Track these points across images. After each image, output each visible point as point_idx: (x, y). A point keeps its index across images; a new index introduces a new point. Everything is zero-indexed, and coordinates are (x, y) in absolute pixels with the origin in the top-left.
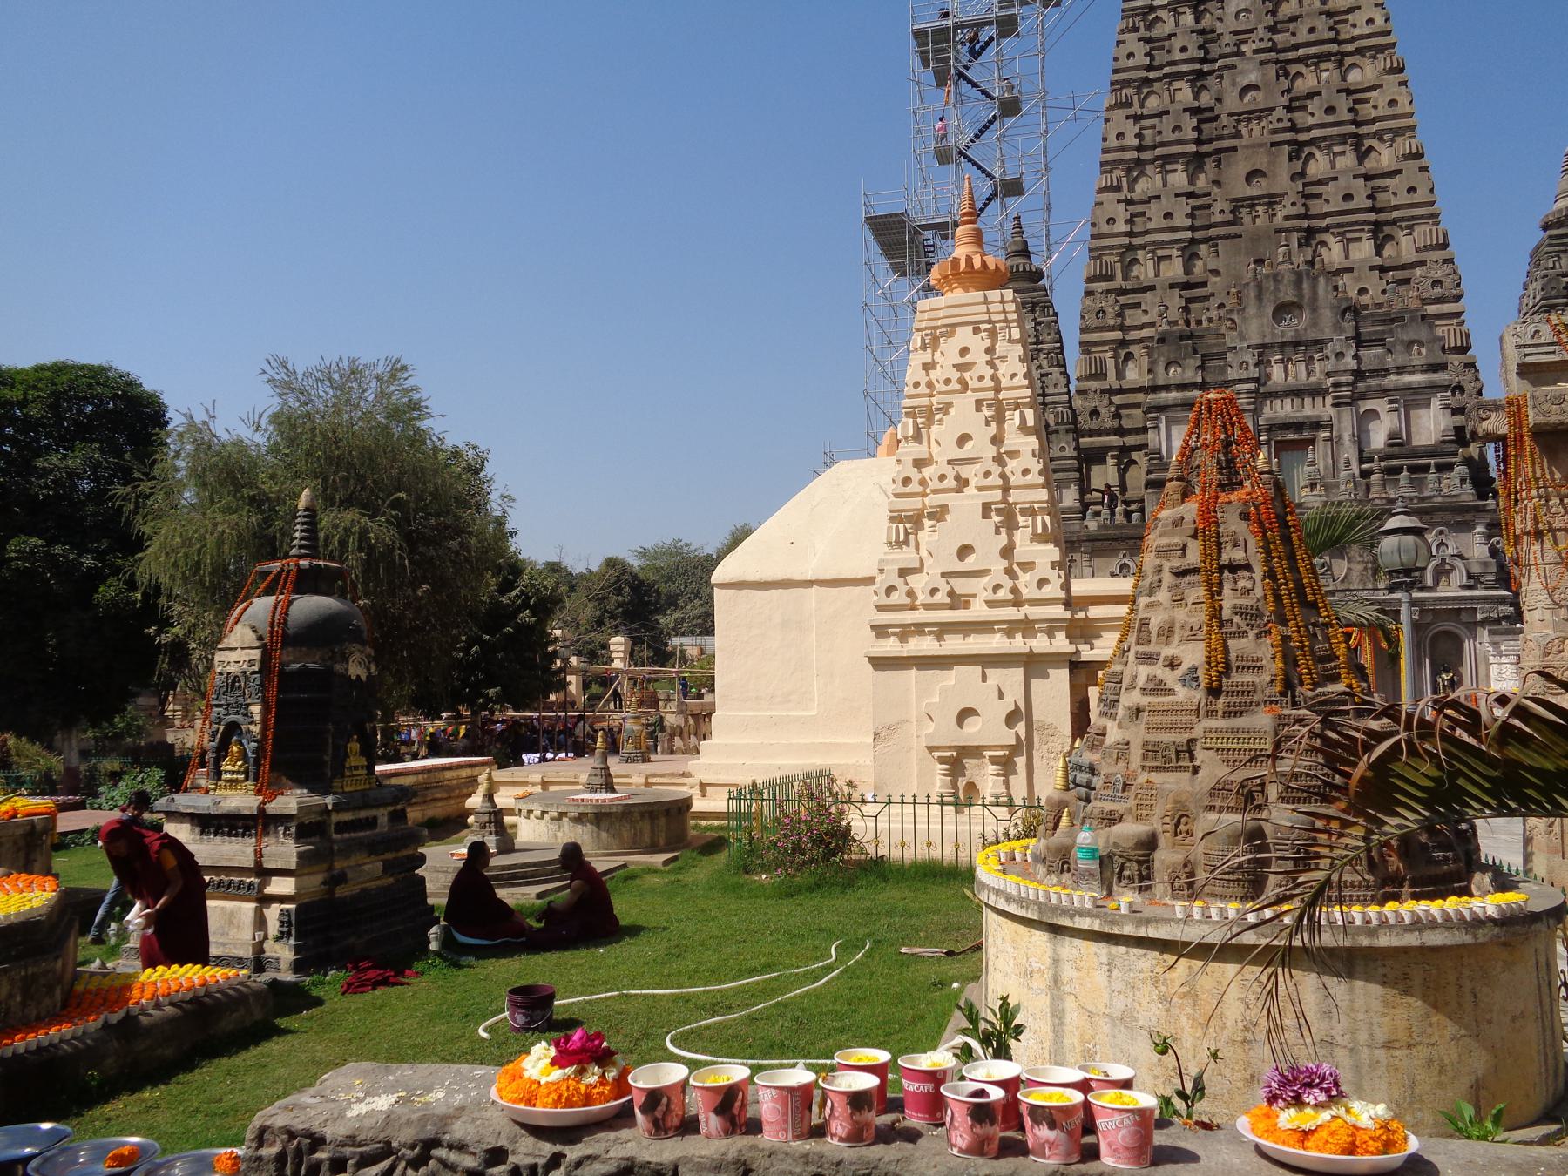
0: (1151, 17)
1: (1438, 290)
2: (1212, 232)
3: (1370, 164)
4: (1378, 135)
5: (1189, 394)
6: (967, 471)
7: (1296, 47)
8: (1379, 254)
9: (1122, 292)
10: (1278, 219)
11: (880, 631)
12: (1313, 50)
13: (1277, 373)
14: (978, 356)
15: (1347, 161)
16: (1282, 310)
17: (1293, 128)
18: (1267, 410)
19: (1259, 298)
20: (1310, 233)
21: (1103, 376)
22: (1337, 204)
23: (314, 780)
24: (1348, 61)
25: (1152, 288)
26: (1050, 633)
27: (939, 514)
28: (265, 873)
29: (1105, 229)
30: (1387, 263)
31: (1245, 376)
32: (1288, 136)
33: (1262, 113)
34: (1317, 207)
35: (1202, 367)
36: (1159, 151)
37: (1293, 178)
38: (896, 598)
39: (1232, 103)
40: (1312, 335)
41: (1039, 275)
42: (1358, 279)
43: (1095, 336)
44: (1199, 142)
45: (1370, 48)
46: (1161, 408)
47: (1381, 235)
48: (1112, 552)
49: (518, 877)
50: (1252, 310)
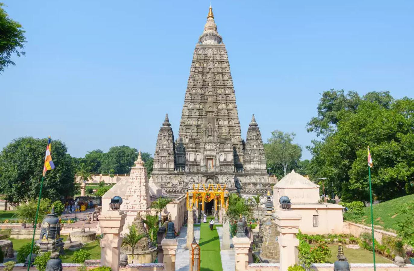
0: (194, 76)
1: (237, 131)
2: (203, 117)
3: (228, 108)
5: (193, 149)
7: (218, 85)
10: (213, 116)
22: (223, 114)
25: (192, 126)
31: (202, 147)
34: (220, 114)
37: (216, 108)
41: (170, 125)
45: (229, 88)
50: (204, 136)
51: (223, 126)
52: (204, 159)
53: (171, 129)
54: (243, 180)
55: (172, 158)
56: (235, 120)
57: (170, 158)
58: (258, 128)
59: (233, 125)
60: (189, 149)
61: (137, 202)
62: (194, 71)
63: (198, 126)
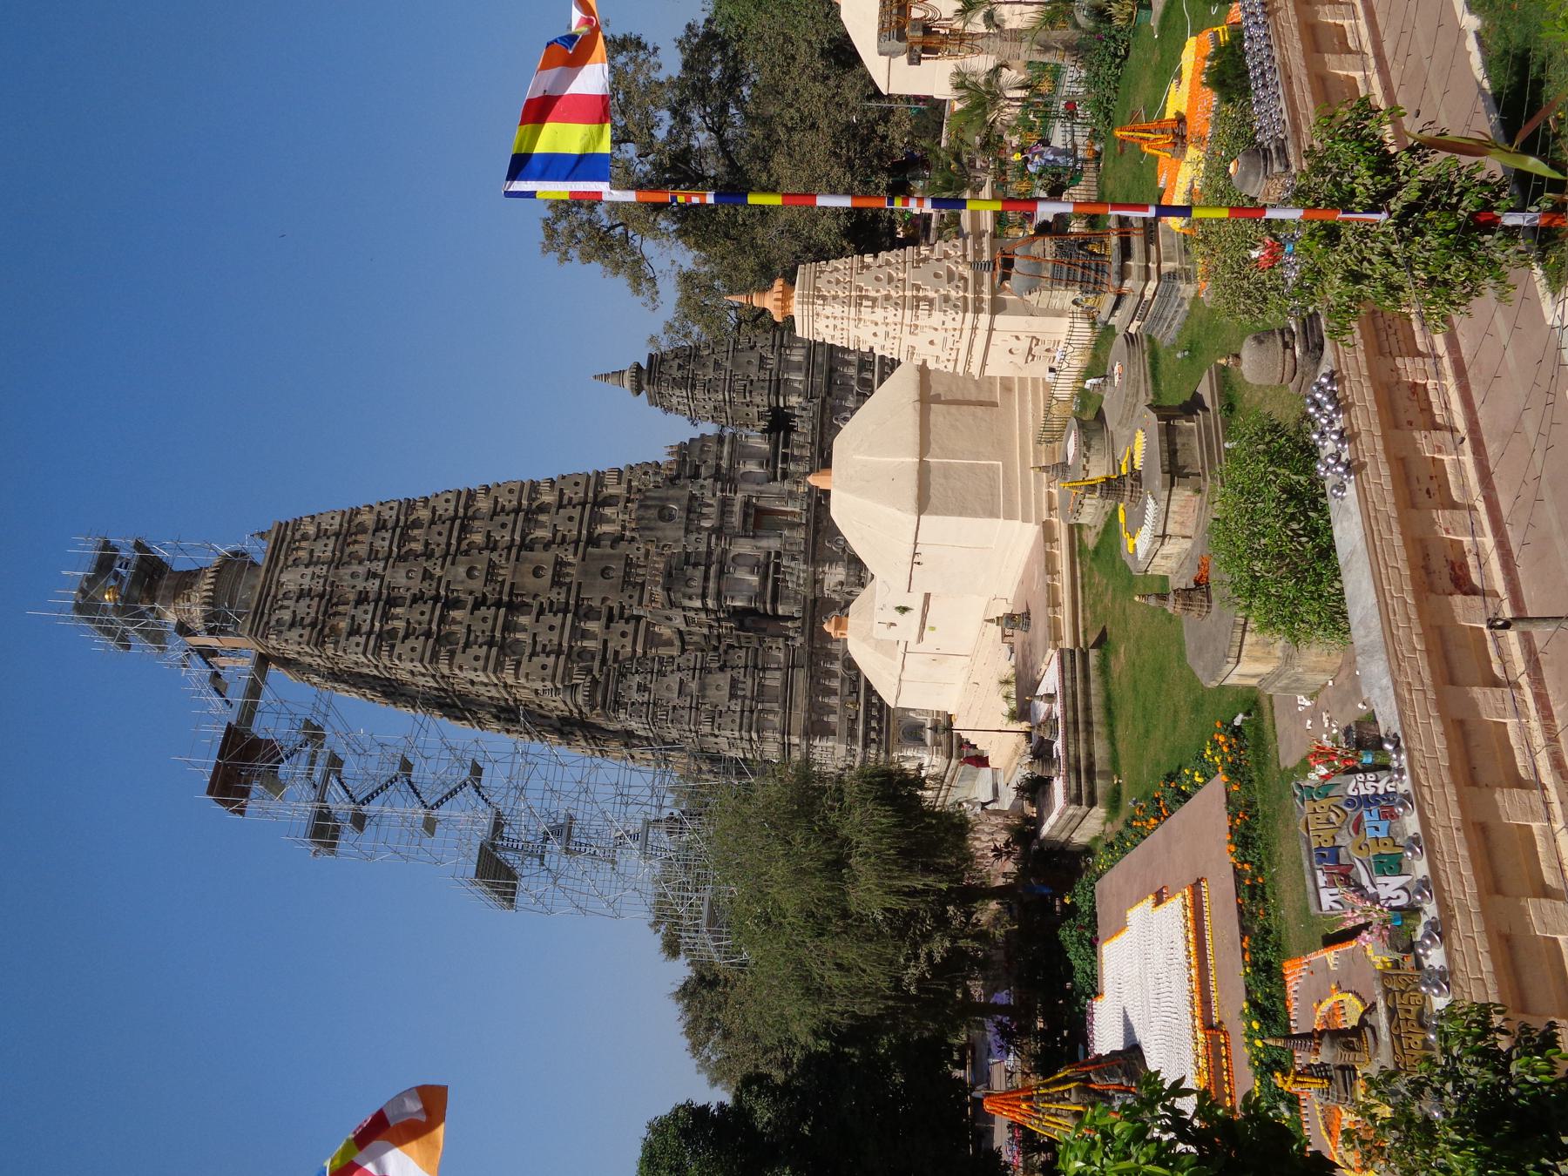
7: (449, 544)
12: (455, 534)
19: (651, 529)
25: (605, 642)
29: (549, 671)
39: (477, 585)
50: (659, 534)
57: (742, 663)
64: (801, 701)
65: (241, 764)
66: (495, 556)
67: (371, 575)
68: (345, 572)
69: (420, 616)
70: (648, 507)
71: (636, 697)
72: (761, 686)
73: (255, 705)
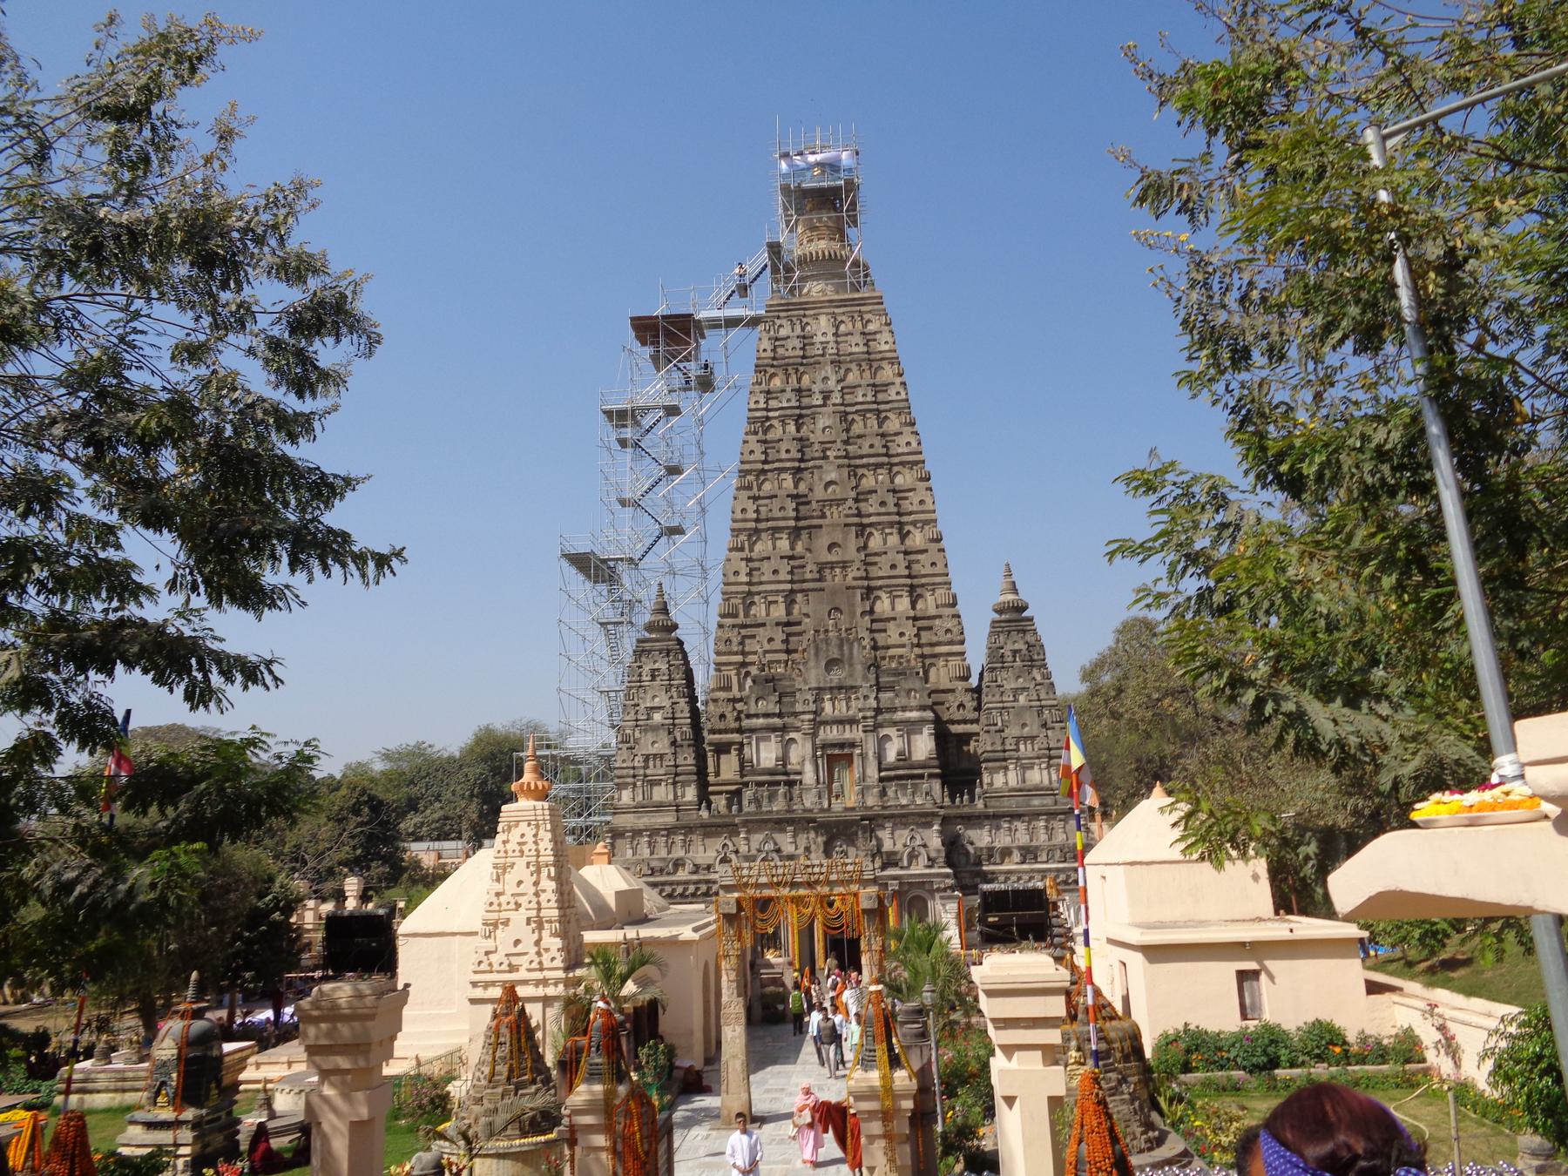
2: (806, 586)
4: (914, 523)
6: (521, 900)
7: (862, 457)
8: (913, 608)
9: (744, 626)
11: (474, 984)
12: (872, 460)
13: (828, 706)
14: (529, 838)
15: (894, 540)
16: (831, 664)
17: (859, 515)
18: (821, 732)
19: (817, 654)
20: (870, 589)
21: (729, 688)
23: (199, 1105)
24: (895, 469)
25: (763, 625)
26: (556, 985)
27: (506, 923)
28: (177, 1146)
29: (732, 579)
30: (919, 614)
32: (856, 520)
33: (839, 502)
35: (779, 702)
36: (770, 524)
37: (858, 550)
38: (483, 967)
39: (819, 493)
40: (849, 683)
42: (899, 626)
43: (724, 659)
44: (797, 519)
46: (752, 730)
47: (915, 594)
48: (718, 835)
49: (281, 1132)
50: (812, 663)
51: (888, 620)
52: (815, 756)
53: (681, 643)
54: (980, 838)
55: (687, 759)
56: (940, 592)
58: (1031, 619)
59: (932, 611)
60: (754, 721)
61: (528, 945)
62: (762, 405)
63: (788, 624)
64: (644, 821)
65: (668, 334)
66: (850, 503)
67: (826, 396)
68: (828, 370)
69: (787, 450)
70: (841, 646)
71: (646, 669)
72: (659, 783)
73: (720, 326)
